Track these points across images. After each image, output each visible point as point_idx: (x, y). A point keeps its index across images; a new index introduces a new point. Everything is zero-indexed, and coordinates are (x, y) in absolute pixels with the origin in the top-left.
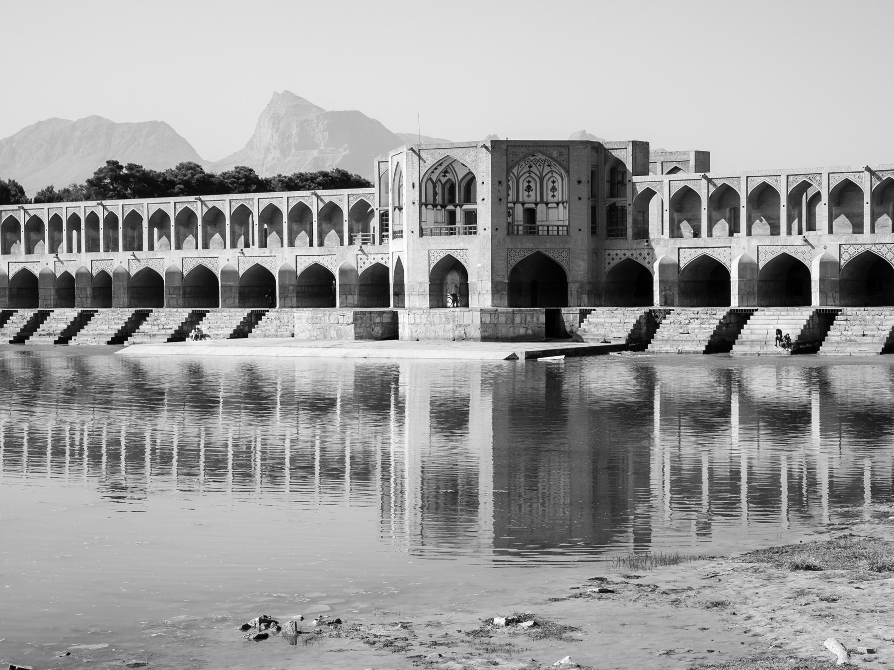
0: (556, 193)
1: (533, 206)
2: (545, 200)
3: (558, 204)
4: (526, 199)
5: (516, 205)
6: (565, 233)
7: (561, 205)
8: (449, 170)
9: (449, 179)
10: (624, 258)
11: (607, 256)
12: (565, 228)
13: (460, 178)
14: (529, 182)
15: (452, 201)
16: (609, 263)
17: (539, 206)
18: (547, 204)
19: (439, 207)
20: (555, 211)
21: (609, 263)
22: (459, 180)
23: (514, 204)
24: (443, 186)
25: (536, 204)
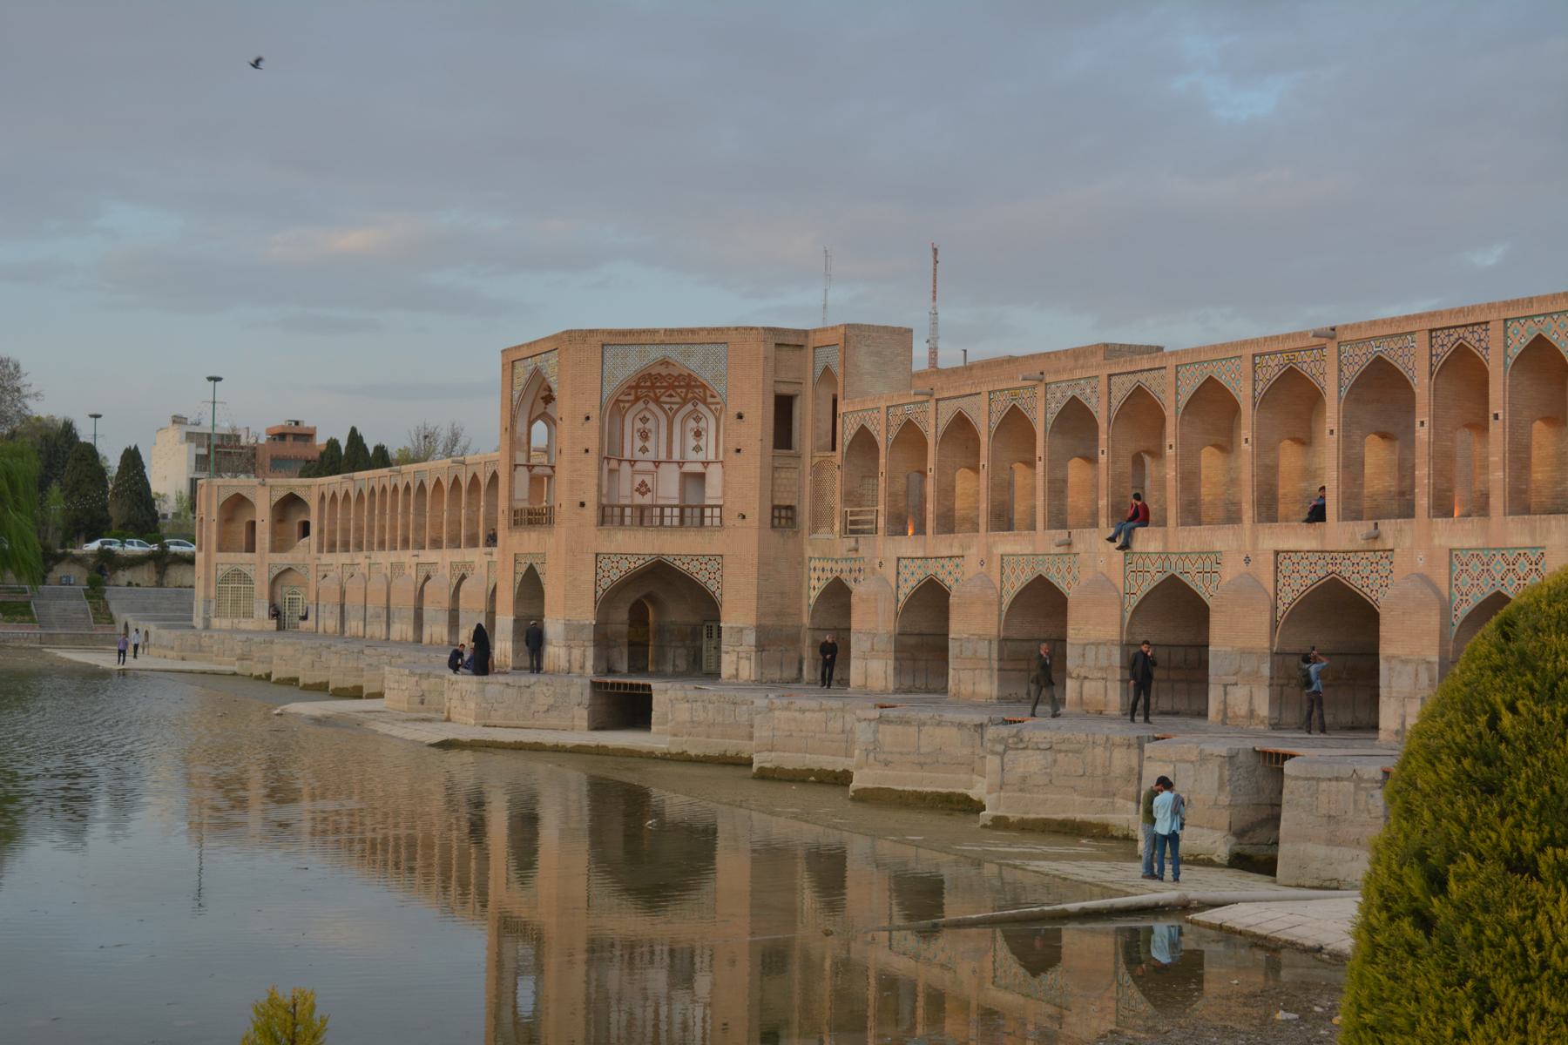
1: (699, 468)
4: (691, 455)
5: (662, 465)
6: (716, 521)
10: (831, 576)
11: (812, 574)
12: (717, 512)
14: (698, 420)
16: (814, 589)
17: (711, 465)
23: (657, 463)
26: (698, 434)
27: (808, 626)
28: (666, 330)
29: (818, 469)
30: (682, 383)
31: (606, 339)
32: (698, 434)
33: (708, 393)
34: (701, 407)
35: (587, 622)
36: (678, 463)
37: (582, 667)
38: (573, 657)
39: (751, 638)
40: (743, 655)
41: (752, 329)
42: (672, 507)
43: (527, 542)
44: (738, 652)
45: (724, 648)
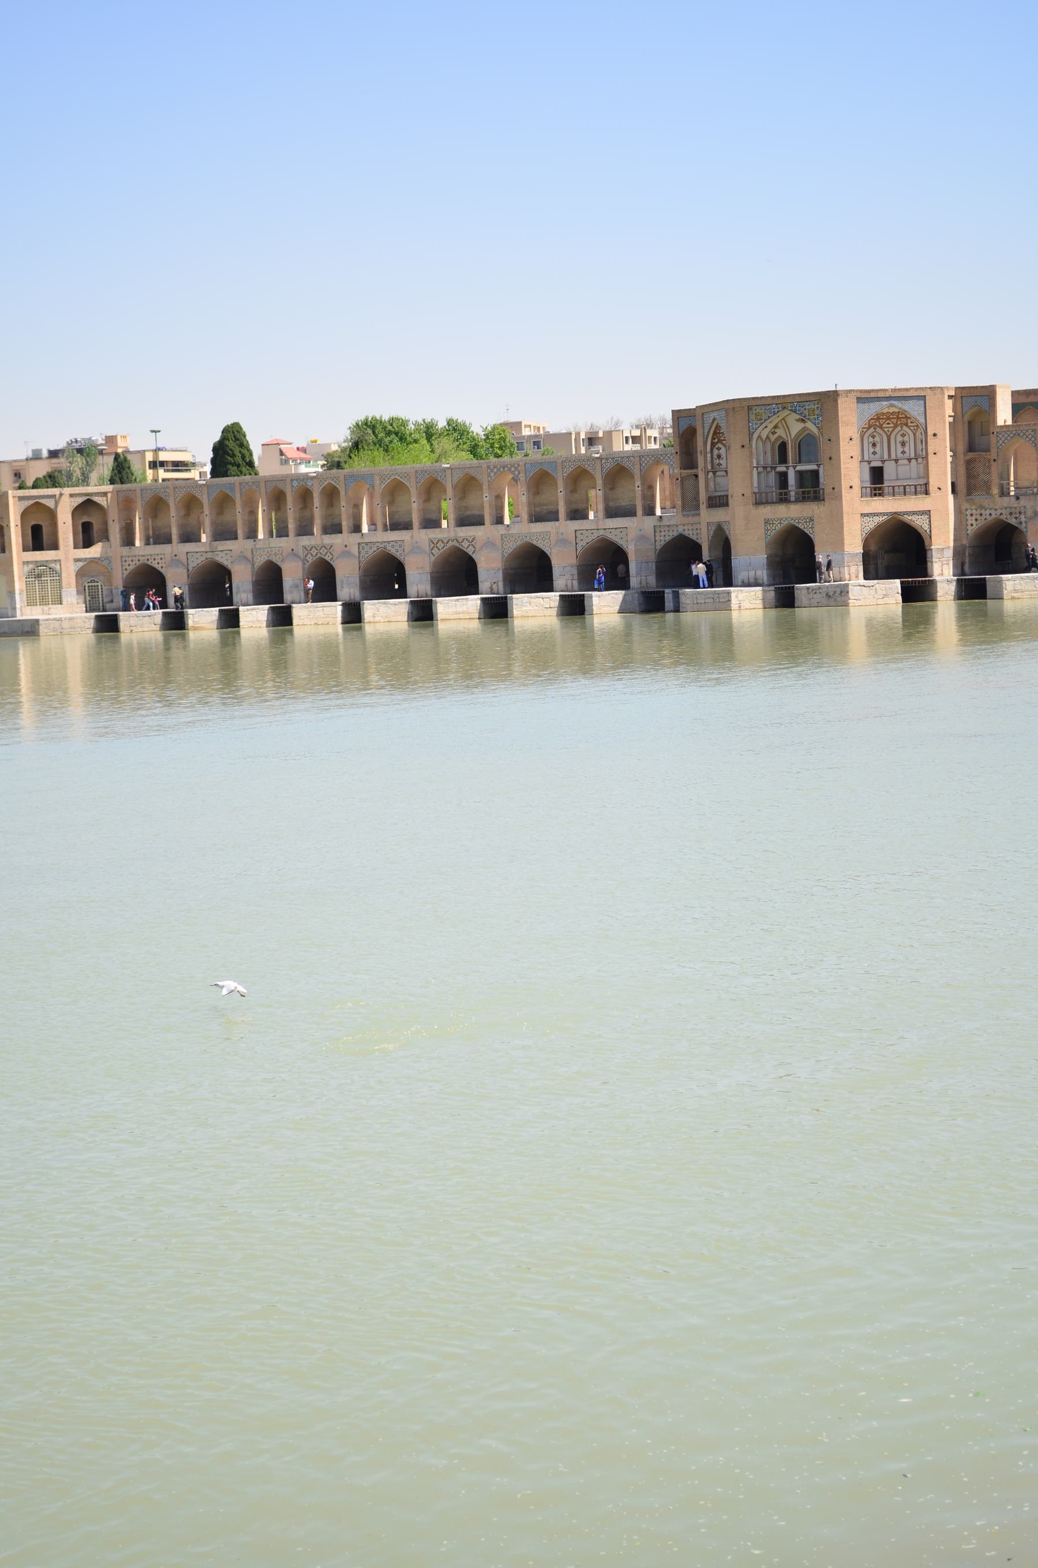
0: (906, 449)
2: (893, 457)
3: (909, 460)
7: (914, 461)
8: (780, 425)
9: (780, 436)
11: (969, 517)
13: (793, 434)
14: (873, 437)
15: (783, 459)
18: (896, 461)
19: (769, 469)
20: (907, 467)
21: (972, 525)
22: (792, 438)
24: (773, 445)
25: (883, 461)
26: (874, 445)
27: (968, 545)
28: (892, 389)
29: (969, 463)
30: (895, 416)
31: (859, 395)
32: (874, 445)
33: (909, 421)
34: (878, 430)
35: (858, 552)
36: (868, 461)
37: (857, 577)
38: (851, 571)
39: (949, 553)
40: (944, 562)
41: (938, 388)
42: (866, 488)
43: (793, 513)
44: (942, 561)
45: (934, 560)
